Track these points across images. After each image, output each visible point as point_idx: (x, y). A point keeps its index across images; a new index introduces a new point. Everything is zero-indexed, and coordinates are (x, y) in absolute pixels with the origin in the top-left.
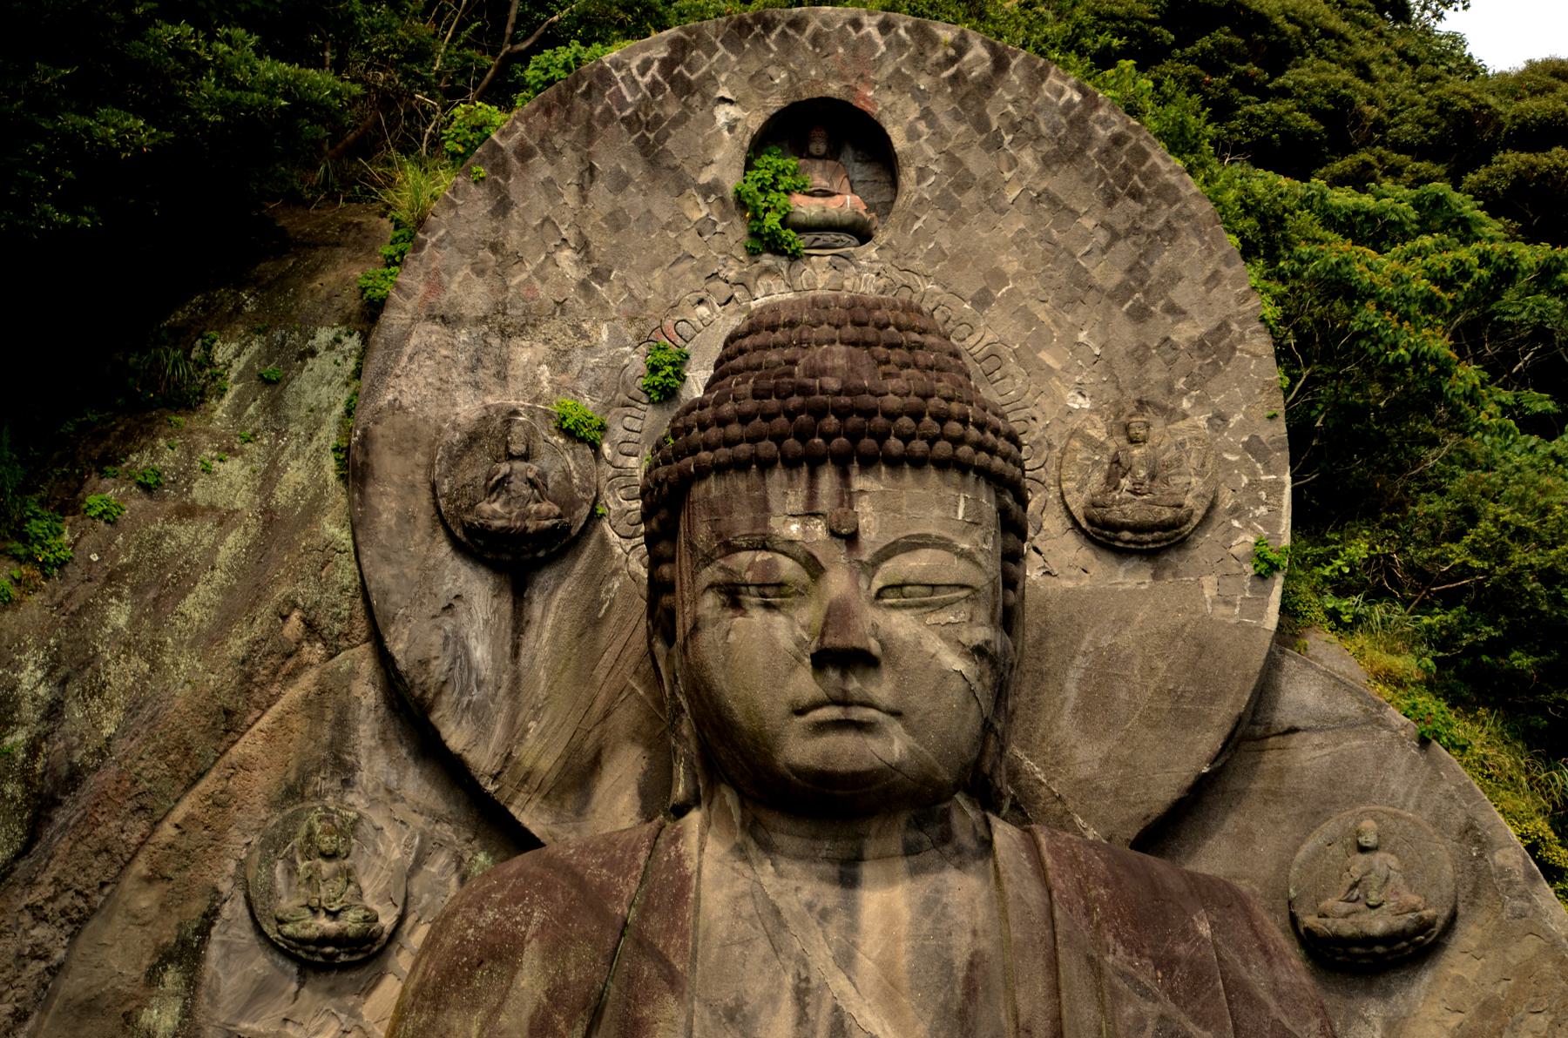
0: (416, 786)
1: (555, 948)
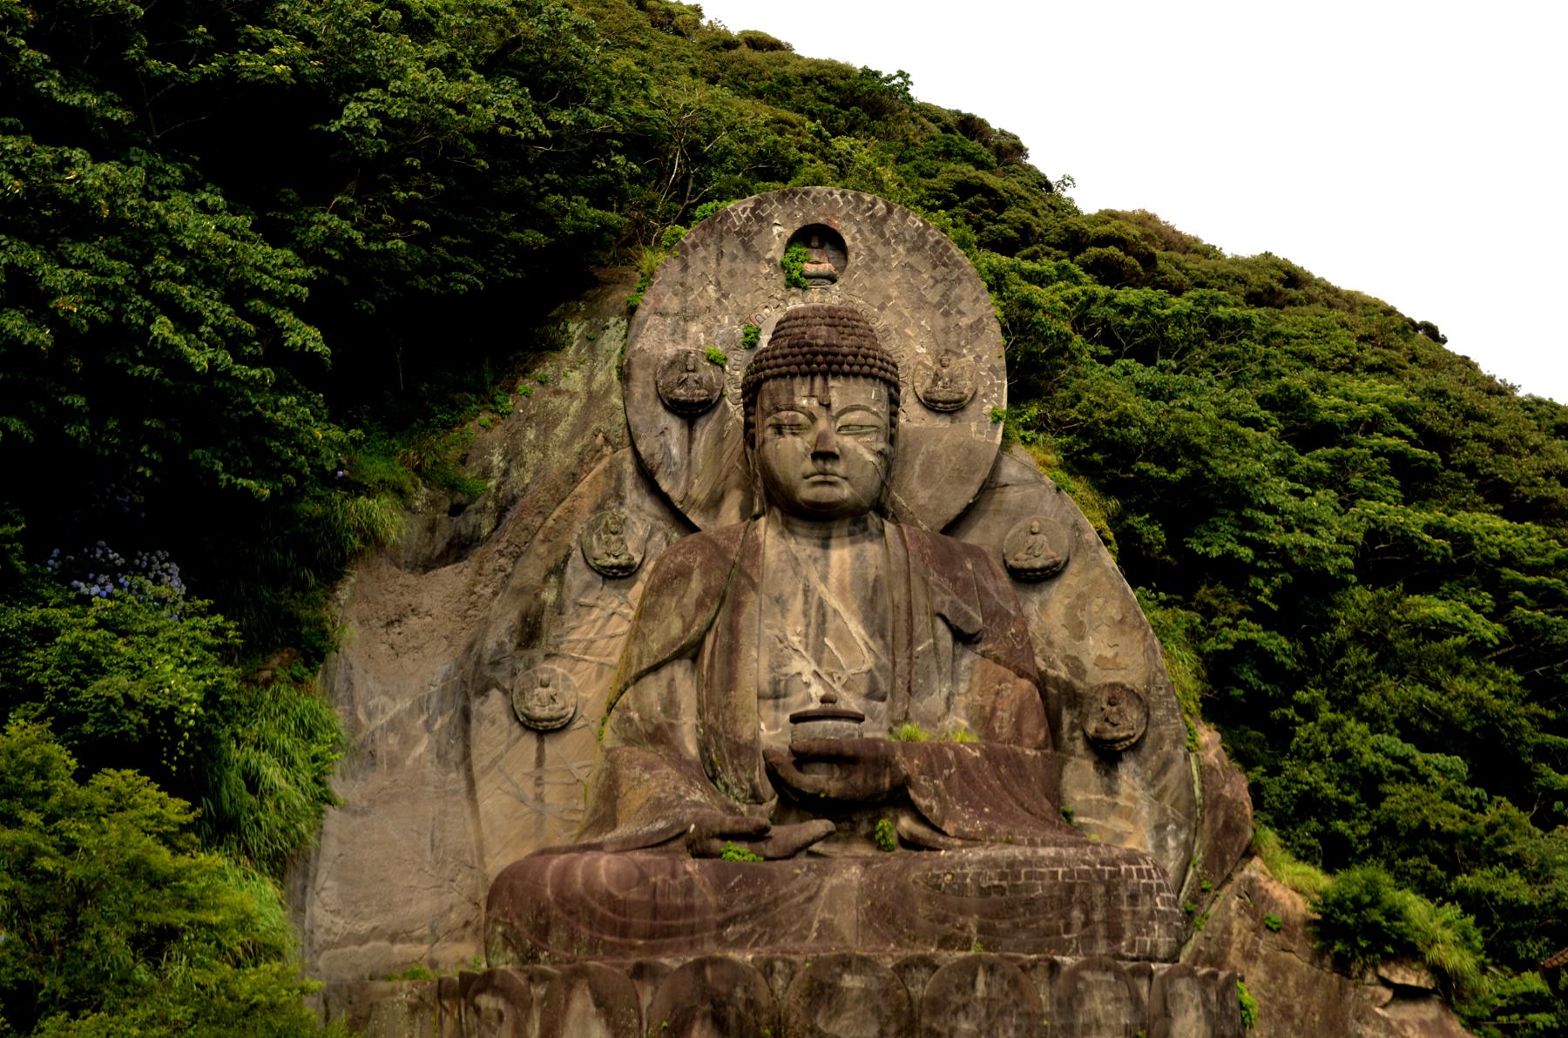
0: (649, 505)
1: (706, 573)
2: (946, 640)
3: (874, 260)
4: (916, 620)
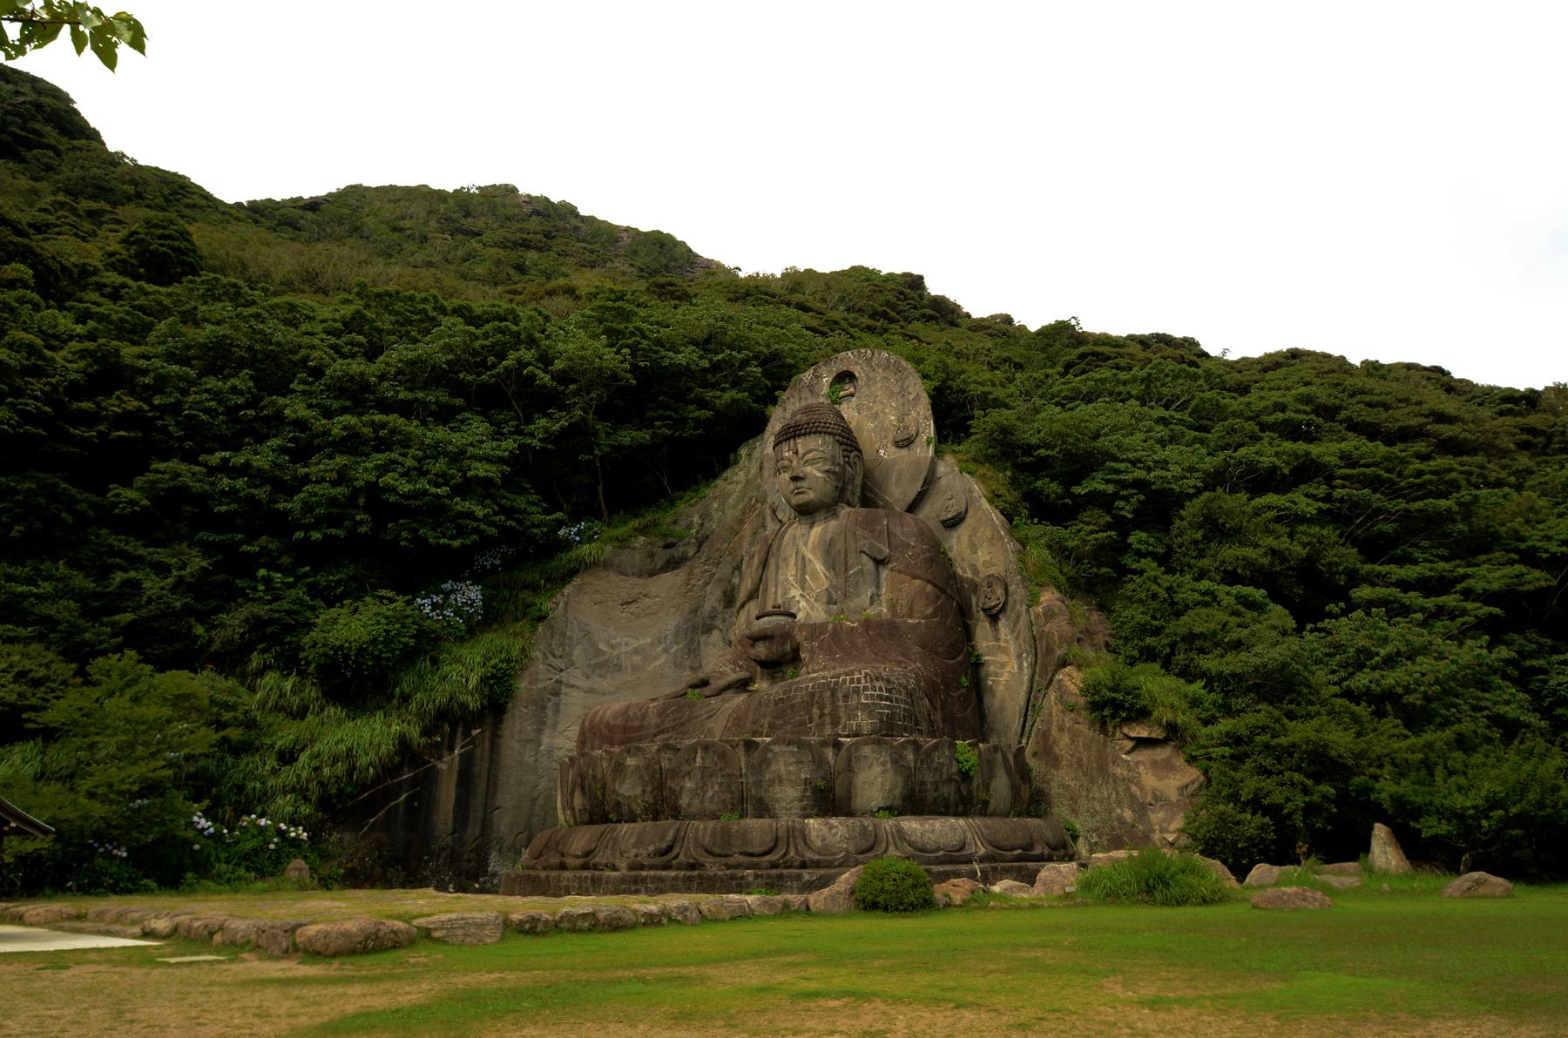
2: (870, 565)
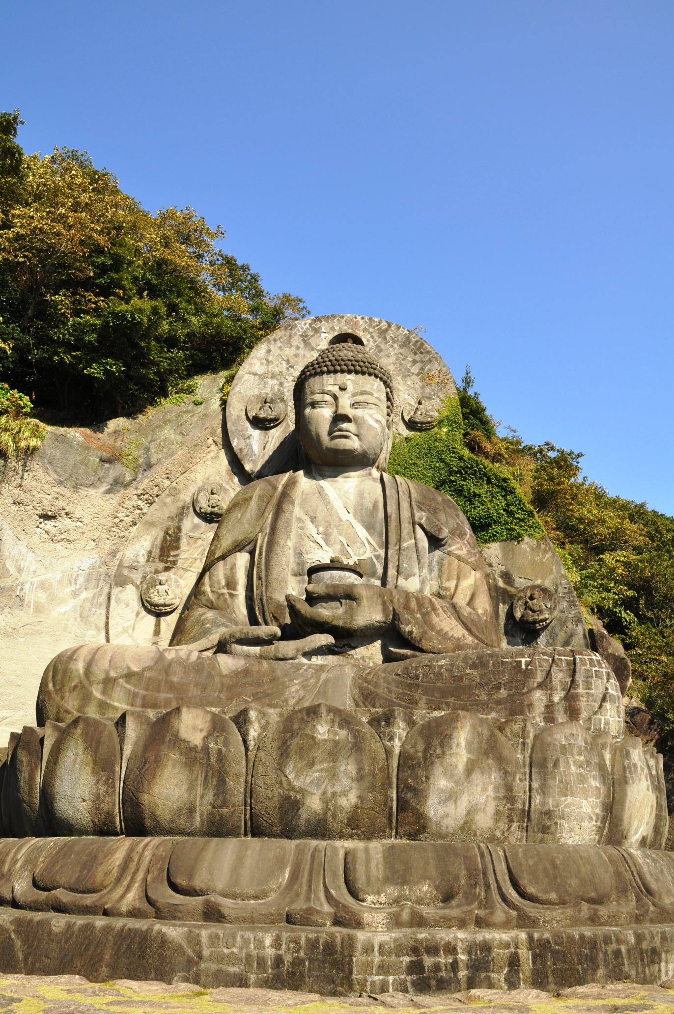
2: (424, 543)
3: (380, 351)
4: (403, 526)
